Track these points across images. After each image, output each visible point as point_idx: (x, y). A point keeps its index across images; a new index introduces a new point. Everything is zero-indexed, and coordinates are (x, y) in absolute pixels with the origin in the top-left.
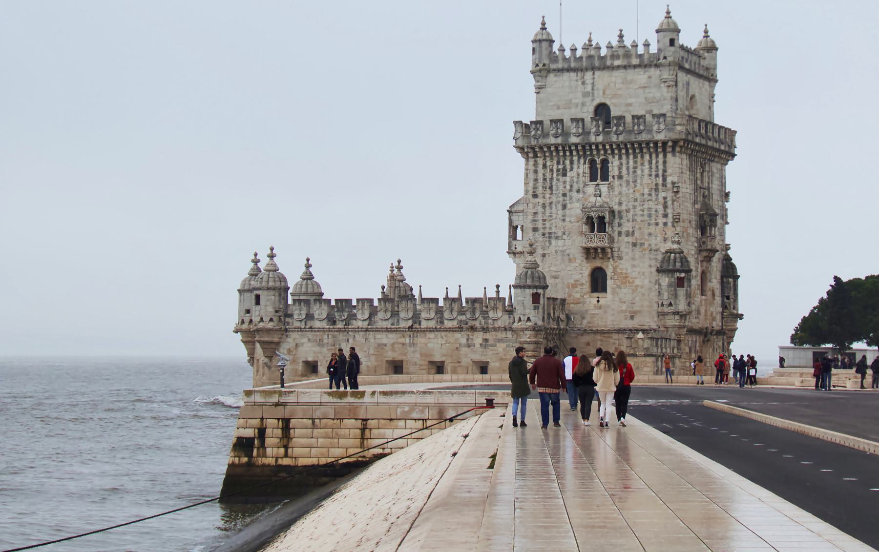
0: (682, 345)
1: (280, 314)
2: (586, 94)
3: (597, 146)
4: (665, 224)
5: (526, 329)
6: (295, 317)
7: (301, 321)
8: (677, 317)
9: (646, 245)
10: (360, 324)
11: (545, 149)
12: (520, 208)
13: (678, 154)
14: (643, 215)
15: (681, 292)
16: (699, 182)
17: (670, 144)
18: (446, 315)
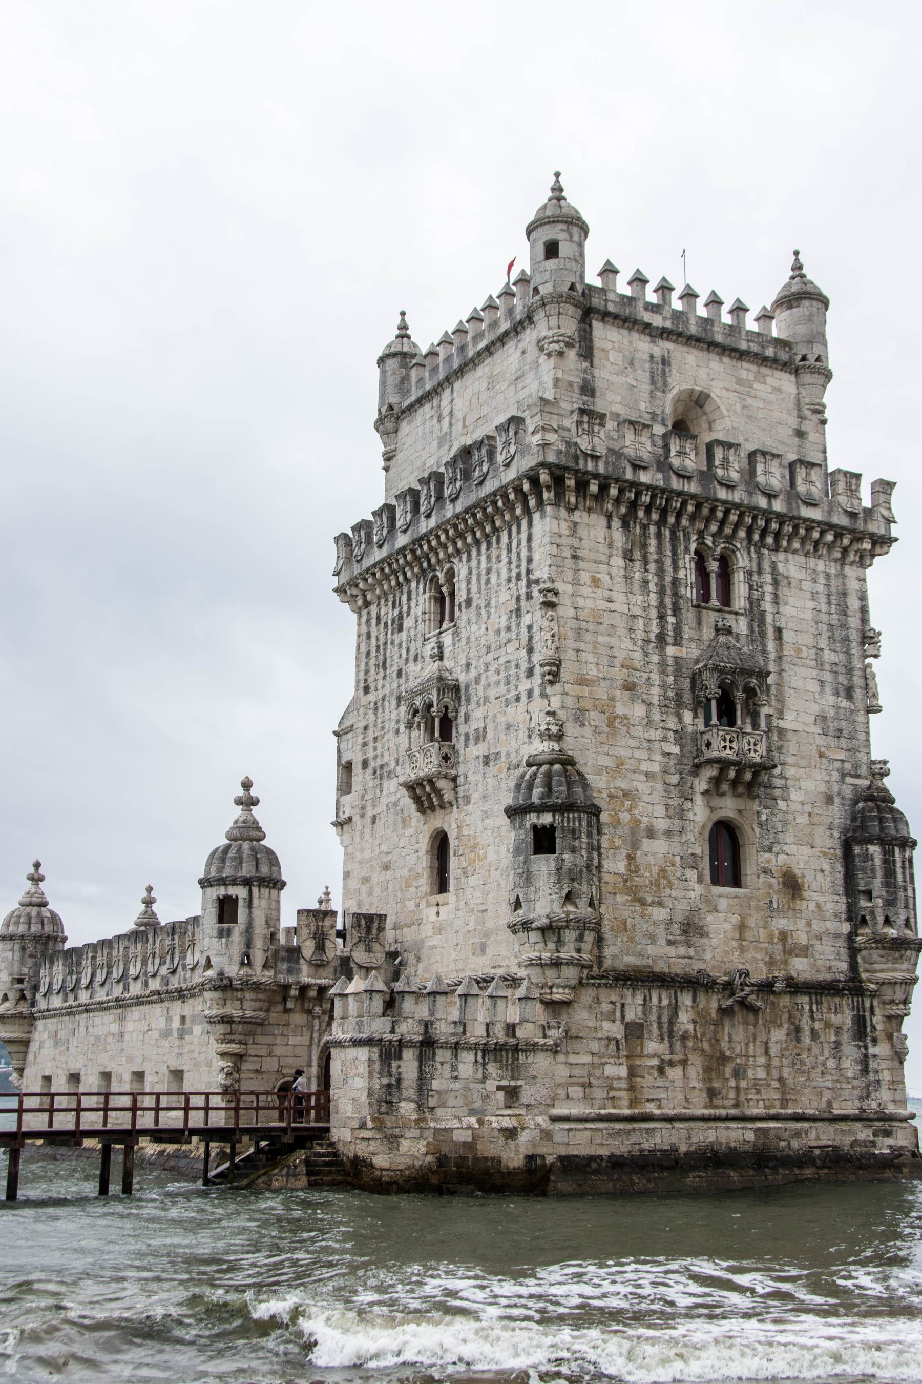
0: (581, 1017)
1: (25, 985)
2: (444, 440)
3: (429, 542)
4: (530, 693)
5: (203, 987)
6: (42, 990)
7: (45, 995)
8: (534, 936)
9: (503, 758)
10: (84, 997)
11: (370, 580)
12: (348, 723)
13: (549, 509)
14: (498, 683)
15: (544, 865)
16: (689, 593)
17: (526, 487)
18: (150, 969)
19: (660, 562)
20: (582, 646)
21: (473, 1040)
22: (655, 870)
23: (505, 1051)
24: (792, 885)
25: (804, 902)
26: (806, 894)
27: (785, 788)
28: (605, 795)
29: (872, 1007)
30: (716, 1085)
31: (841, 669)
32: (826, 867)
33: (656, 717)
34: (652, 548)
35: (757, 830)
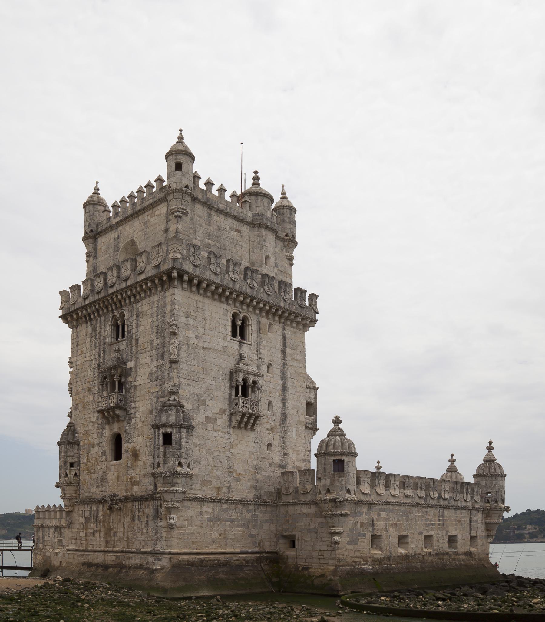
19: (100, 332)
20: (78, 379)
21: (50, 525)
22: (94, 459)
23: (58, 529)
24: (135, 455)
25: (139, 462)
26: (140, 458)
27: (135, 413)
28: (82, 435)
29: (161, 505)
30: (108, 539)
31: (160, 346)
32: (148, 444)
33: (96, 398)
34: (98, 328)
35: (124, 434)
